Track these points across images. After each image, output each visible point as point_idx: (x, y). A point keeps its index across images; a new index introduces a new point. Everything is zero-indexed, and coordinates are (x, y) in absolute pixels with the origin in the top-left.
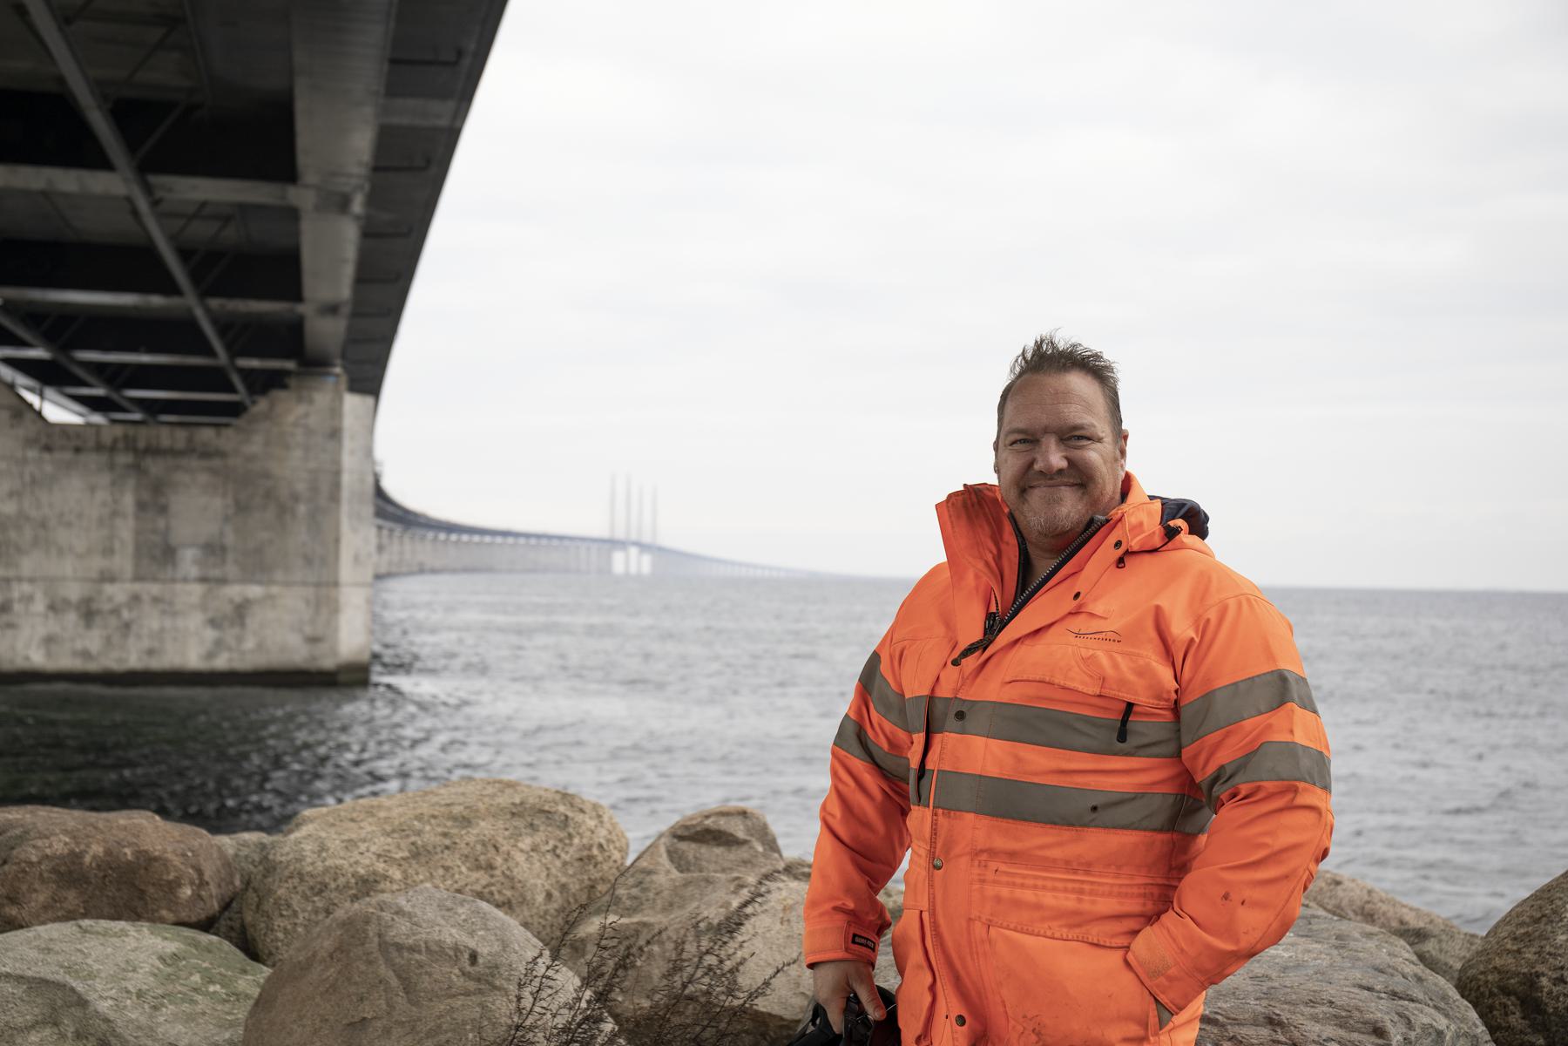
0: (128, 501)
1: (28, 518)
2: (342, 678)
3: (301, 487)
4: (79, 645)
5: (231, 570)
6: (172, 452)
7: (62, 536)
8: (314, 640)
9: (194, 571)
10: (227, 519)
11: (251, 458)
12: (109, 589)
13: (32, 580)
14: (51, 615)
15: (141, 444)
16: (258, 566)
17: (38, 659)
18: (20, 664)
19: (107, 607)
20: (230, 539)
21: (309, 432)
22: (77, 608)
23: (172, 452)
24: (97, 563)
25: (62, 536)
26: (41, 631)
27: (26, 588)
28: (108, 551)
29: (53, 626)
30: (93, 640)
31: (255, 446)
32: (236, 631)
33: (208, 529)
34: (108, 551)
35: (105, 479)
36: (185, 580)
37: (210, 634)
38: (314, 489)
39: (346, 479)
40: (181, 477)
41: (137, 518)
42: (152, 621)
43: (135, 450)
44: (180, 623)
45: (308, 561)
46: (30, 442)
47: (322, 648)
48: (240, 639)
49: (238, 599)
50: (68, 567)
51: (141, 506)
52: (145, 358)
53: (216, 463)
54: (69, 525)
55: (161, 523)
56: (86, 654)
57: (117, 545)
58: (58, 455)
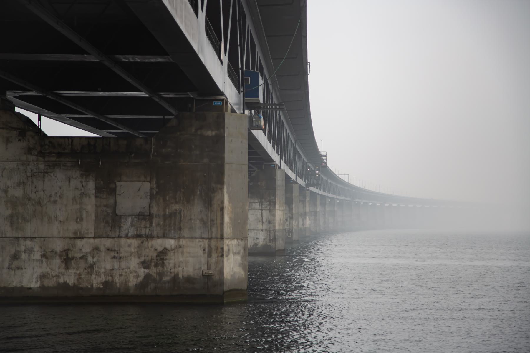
0: (91, 185)
1: (29, 199)
5: (157, 231)
10: (152, 197)
13: (32, 239)
14: (44, 260)
19: (79, 255)
20: (154, 210)
22: (60, 256)
24: (73, 227)
26: (39, 271)
27: (29, 243)
28: (79, 219)
30: (70, 278)
34: (79, 219)
35: (76, 173)
36: (127, 236)
49: (160, 249)
51: (98, 190)
54: (55, 202)
57: (84, 215)
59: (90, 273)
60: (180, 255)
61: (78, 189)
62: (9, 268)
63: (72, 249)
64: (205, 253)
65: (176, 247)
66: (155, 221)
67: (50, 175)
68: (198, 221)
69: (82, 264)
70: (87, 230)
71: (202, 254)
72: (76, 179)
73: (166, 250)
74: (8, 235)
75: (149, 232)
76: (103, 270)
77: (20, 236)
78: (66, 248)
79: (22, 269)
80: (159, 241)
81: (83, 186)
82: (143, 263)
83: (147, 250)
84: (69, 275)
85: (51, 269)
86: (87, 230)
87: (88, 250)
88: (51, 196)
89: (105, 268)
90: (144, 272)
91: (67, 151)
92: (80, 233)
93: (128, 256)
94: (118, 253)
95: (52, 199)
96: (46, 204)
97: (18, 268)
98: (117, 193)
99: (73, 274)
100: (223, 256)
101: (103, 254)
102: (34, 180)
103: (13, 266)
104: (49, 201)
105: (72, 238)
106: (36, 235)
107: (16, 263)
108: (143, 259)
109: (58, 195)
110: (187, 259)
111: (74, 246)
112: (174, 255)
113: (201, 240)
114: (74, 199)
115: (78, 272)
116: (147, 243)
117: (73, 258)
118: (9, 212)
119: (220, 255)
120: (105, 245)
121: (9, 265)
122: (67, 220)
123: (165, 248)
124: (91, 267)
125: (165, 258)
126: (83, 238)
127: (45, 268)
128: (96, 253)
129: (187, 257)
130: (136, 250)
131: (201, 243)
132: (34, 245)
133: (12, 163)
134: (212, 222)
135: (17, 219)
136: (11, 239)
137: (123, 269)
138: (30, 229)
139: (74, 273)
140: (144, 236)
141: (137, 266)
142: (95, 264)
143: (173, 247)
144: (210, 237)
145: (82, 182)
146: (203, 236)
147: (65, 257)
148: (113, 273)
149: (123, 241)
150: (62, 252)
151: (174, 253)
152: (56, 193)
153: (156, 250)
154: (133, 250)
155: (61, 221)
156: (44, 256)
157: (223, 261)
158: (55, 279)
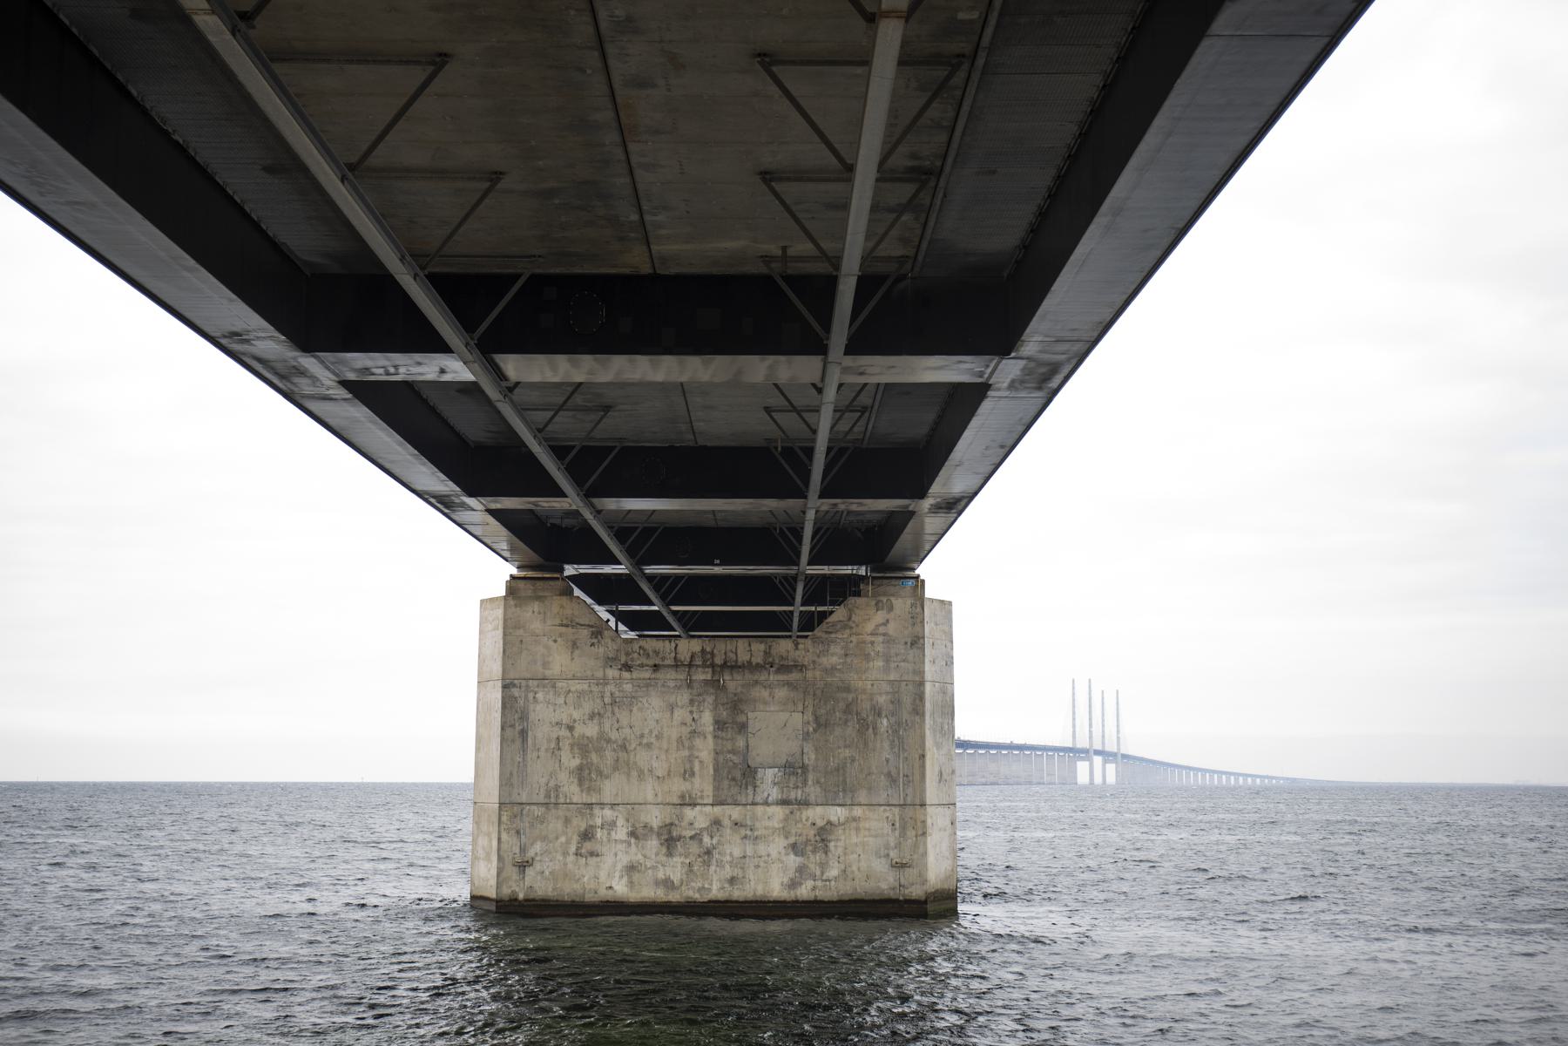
0: (707, 718)
1: (609, 741)
2: (930, 908)
3: (882, 700)
4: (661, 875)
5: (813, 791)
6: (750, 667)
7: (642, 758)
8: (900, 866)
9: (775, 794)
10: (806, 736)
11: (831, 670)
12: (689, 813)
13: (613, 805)
14: (633, 840)
15: (718, 661)
16: (840, 787)
17: (621, 889)
18: (604, 894)
19: (689, 833)
20: (810, 758)
21: (889, 640)
22: (659, 835)
23: (750, 667)
24: (678, 786)
25: (642, 758)
26: (624, 860)
27: (608, 813)
28: (688, 774)
29: (635, 855)
30: (674, 869)
31: (833, 659)
32: (819, 856)
33: (788, 747)
34: (688, 774)
35: (683, 697)
36: (766, 803)
37: (793, 861)
38: (896, 702)
39: (928, 687)
40: (760, 693)
41: (715, 737)
42: (733, 847)
43: (713, 666)
44: (762, 848)
45: (892, 780)
46: (609, 661)
47: (910, 875)
48: (823, 866)
49: (820, 823)
50: (648, 791)
51: (720, 725)
52: (718, 570)
53: (794, 676)
54: (649, 746)
55: (741, 743)
56: (667, 884)
57: (697, 768)
58: (635, 674)
59: (707, 864)
60: (853, 832)
61: (686, 724)
62: (576, 854)
63: (677, 822)
64: (895, 829)
65: (847, 820)
66: (811, 777)
67: (641, 702)
68: (883, 777)
69: (694, 848)
70: (702, 791)
71: (890, 833)
72: (682, 707)
73: (831, 824)
74: (575, 801)
75: (802, 795)
76: (728, 858)
77: (594, 801)
78: (668, 821)
79: (598, 855)
80: (819, 809)
81: (693, 719)
82: (794, 847)
83: (800, 825)
84: (673, 866)
85: (645, 857)
86: (702, 791)
87: (703, 826)
88: (642, 736)
89: (731, 854)
90: (794, 861)
91: (668, 662)
92: (690, 796)
93: (769, 836)
94: (751, 830)
95: (645, 741)
96: (635, 749)
97: (592, 854)
98: (750, 730)
99: (679, 865)
100: (924, 834)
101: (728, 831)
102: (616, 710)
103: (583, 851)
104: (640, 744)
105: (677, 805)
106: (619, 800)
107: (588, 846)
108: (792, 840)
109: (654, 735)
110: (865, 839)
111: (680, 817)
112: (844, 833)
113: (888, 808)
114: (680, 740)
115: (688, 861)
116: (798, 813)
117: (679, 838)
118: (577, 762)
119: (920, 832)
120: (730, 816)
121: (577, 849)
122: (669, 775)
123: (829, 823)
124: (708, 852)
125: (830, 838)
126: (695, 805)
127: (635, 855)
128: (715, 830)
129: (865, 836)
130: (781, 825)
131: (888, 814)
132: (617, 817)
133: (581, 681)
134: (905, 778)
135: (590, 774)
136: (579, 806)
137: (760, 857)
138: (610, 789)
139: (682, 863)
140: (794, 801)
141: (783, 851)
142: (714, 848)
143: (842, 820)
144: (902, 802)
145: (691, 712)
146: (890, 803)
147: (666, 837)
148: (744, 864)
149: (760, 809)
150: (661, 827)
151: (844, 829)
152: (651, 731)
153: (814, 824)
154: (776, 825)
155: (658, 777)
156: (633, 834)
157: (925, 844)
158: (650, 871)
